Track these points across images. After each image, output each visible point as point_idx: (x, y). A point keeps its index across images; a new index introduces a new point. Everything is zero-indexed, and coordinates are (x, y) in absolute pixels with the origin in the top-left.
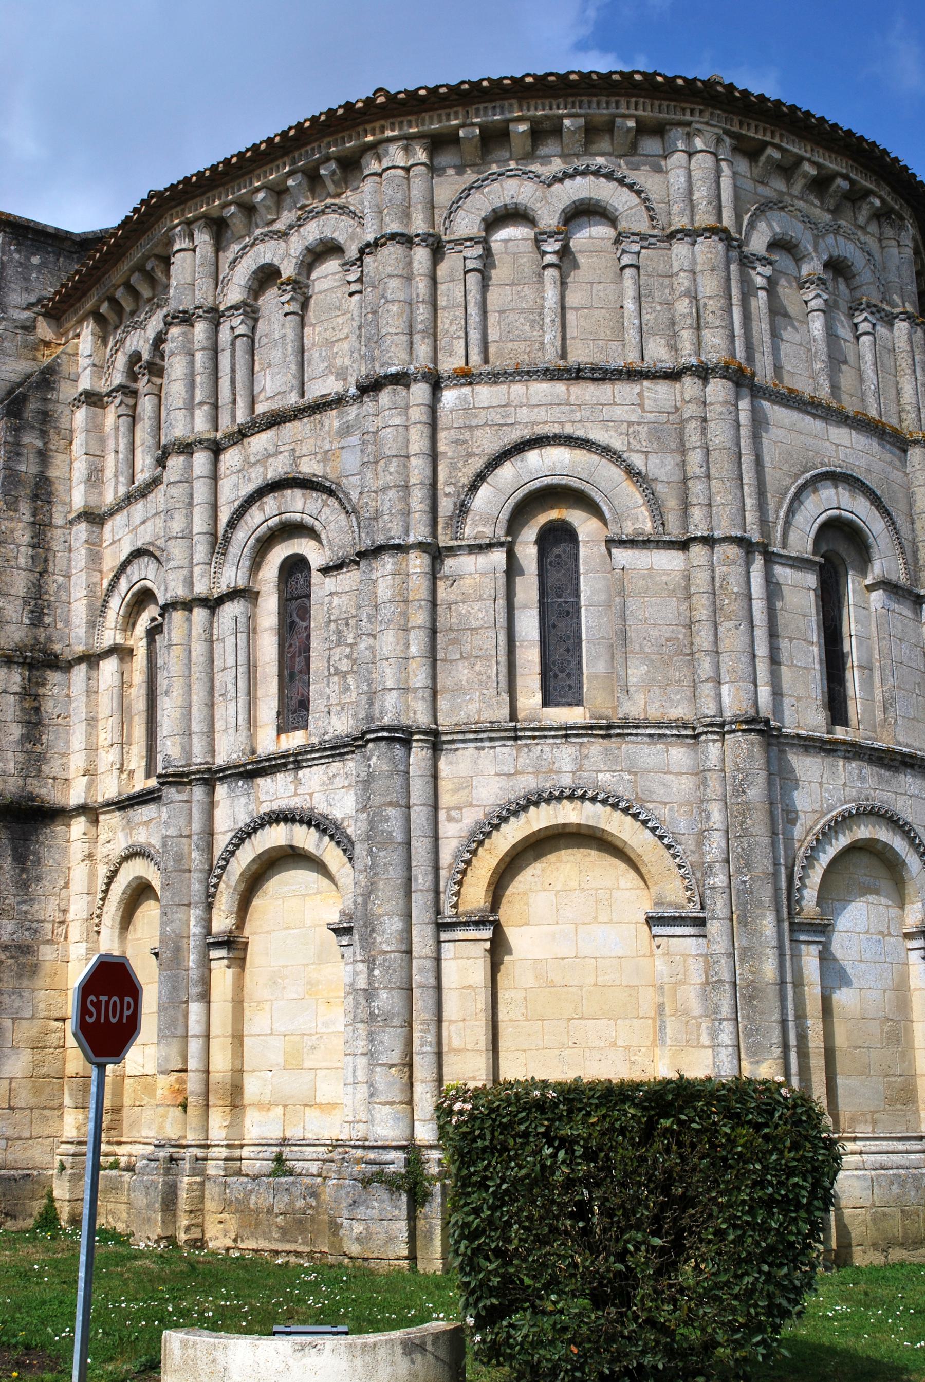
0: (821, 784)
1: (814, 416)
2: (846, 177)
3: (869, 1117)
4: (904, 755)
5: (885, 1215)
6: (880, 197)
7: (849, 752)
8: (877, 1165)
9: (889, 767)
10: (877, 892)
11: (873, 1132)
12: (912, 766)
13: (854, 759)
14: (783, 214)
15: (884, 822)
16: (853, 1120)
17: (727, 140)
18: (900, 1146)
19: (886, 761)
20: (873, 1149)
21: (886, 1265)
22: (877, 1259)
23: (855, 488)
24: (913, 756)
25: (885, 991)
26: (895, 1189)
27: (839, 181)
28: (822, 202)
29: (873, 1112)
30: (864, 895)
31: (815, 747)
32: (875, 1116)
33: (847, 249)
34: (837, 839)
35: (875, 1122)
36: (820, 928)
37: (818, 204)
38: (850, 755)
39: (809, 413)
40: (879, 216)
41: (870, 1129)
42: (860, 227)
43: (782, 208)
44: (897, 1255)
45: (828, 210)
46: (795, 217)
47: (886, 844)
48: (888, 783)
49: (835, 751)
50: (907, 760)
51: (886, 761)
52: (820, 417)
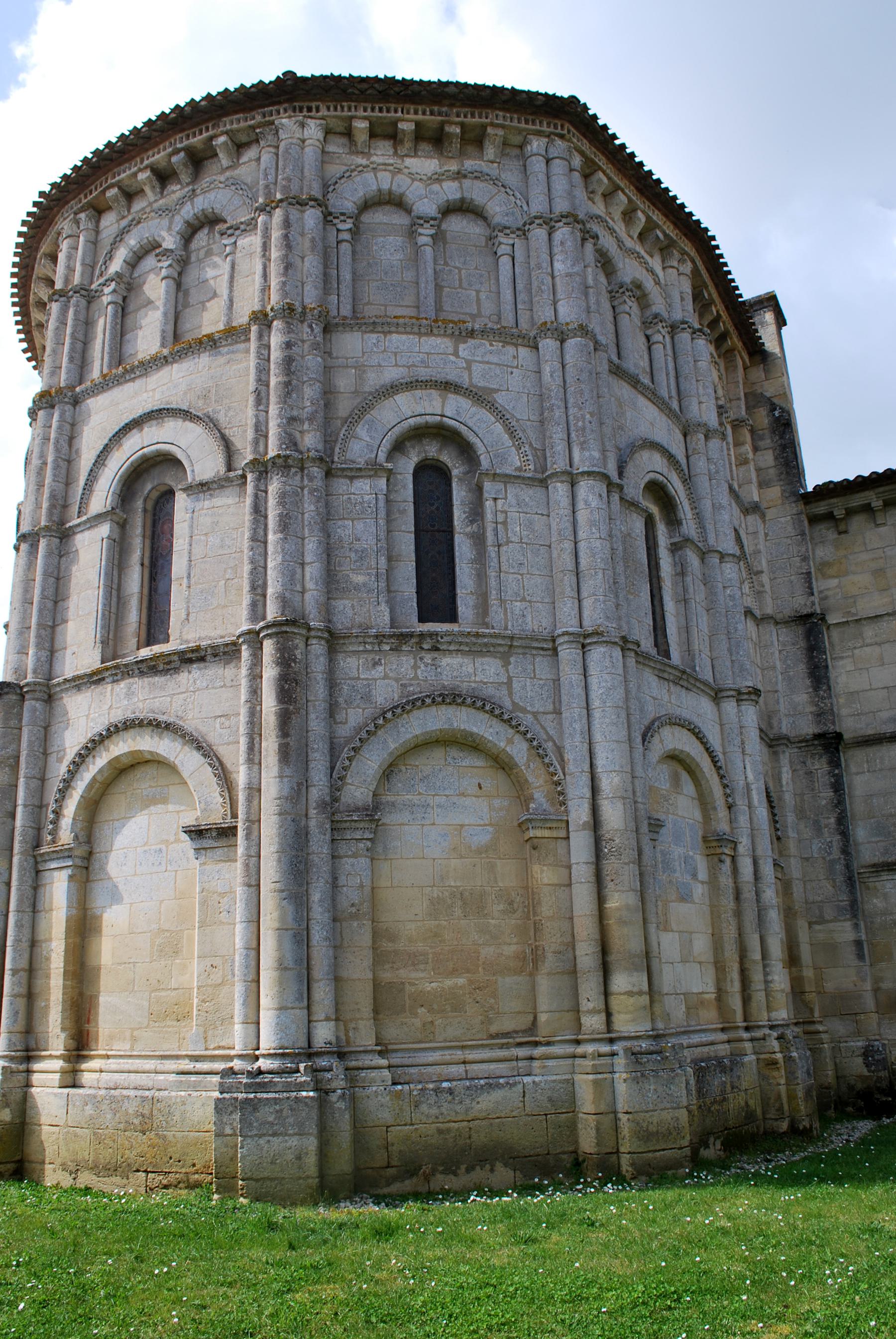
0: (88, 716)
1: (133, 380)
2: (176, 152)
3: (128, 1034)
4: (183, 652)
5: (76, 1135)
6: (222, 133)
7: (116, 674)
8: (112, 1085)
9: (165, 672)
10: (164, 801)
11: (132, 1049)
12: (202, 659)
13: (122, 679)
14: (140, 226)
15: (132, 732)
16: (112, 1037)
17: (82, 216)
18: (150, 1064)
19: (161, 667)
20: (127, 1067)
21: (73, 1189)
22: (66, 1181)
23: (162, 418)
24: (197, 649)
25: (161, 902)
26: (89, 1110)
27: (174, 159)
28: (179, 182)
29: (133, 1029)
30: (147, 806)
31: (85, 683)
32: (136, 1033)
33: (201, 203)
34: (94, 764)
35: (134, 1040)
36: (66, 854)
37: (179, 186)
38: (119, 677)
39: (129, 381)
40: (239, 147)
41: (128, 1047)
42: (227, 168)
43: (139, 222)
44: (86, 1179)
45: (188, 184)
46: (152, 218)
47: (132, 753)
48: (162, 688)
49: (103, 679)
50: (189, 655)
51: (161, 667)
52: (140, 376)
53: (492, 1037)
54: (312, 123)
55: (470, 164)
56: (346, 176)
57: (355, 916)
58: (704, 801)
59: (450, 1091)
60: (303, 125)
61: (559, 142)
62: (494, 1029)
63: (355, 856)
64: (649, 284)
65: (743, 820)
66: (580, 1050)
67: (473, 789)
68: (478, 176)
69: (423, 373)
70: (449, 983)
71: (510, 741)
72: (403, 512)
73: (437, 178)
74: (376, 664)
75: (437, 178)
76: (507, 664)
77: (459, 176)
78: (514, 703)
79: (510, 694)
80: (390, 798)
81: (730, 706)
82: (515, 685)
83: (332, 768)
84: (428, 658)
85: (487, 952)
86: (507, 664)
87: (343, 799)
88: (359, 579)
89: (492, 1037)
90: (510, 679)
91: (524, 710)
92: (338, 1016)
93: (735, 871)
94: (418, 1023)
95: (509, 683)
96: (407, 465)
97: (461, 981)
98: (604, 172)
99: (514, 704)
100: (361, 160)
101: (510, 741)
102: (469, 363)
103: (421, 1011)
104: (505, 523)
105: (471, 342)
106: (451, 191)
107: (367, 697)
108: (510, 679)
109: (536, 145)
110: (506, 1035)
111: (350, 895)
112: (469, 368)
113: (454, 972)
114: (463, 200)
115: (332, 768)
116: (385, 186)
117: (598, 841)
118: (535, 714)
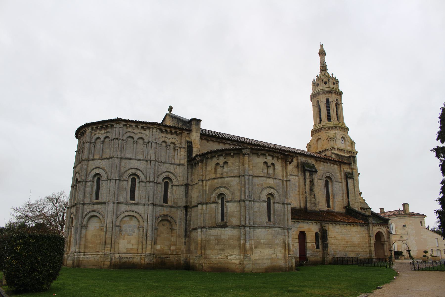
53: (96, 252)
54: (90, 129)
55: (108, 130)
56: (94, 135)
57: (83, 237)
58: (138, 221)
59: (87, 257)
60: (89, 129)
61: (117, 125)
62: (96, 251)
63: (84, 230)
64: (143, 136)
65: (146, 223)
66: (138, 255)
67: (98, 222)
68: (108, 132)
69: (97, 166)
70: (92, 245)
71: (100, 216)
72: (95, 185)
73: (104, 133)
74: (88, 207)
75: (104, 133)
76: (101, 206)
77: (106, 133)
78: (101, 211)
79: (101, 210)
80: (89, 223)
81: (146, 206)
82: (102, 209)
83: (82, 219)
84: (93, 205)
85: (97, 242)
86: (101, 206)
87: (83, 223)
88: (87, 196)
89: (96, 252)
90: (101, 208)
91: (102, 212)
92: (80, 248)
93: (143, 232)
94: (89, 249)
95: (101, 208)
96: (96, 179)
97: (93, 245)
98: (128, 124)
99: (101, 211)
100: (96, 133)
101: (100, 216)
102: (102, 163)
103: (89, 248)
104: (103, 187)
105: (103, 160)
106: (105, 135)
107: (86, 211)
108: (101, 208)
109: (115, 126)
110: (97, 252)
111: (82, 235)
112: (102, 164)
113: (93, 244)
114: (107, 136)
115: (82, 219)
116: (98, 136)
117: (106, 229)
118: (104, 212)
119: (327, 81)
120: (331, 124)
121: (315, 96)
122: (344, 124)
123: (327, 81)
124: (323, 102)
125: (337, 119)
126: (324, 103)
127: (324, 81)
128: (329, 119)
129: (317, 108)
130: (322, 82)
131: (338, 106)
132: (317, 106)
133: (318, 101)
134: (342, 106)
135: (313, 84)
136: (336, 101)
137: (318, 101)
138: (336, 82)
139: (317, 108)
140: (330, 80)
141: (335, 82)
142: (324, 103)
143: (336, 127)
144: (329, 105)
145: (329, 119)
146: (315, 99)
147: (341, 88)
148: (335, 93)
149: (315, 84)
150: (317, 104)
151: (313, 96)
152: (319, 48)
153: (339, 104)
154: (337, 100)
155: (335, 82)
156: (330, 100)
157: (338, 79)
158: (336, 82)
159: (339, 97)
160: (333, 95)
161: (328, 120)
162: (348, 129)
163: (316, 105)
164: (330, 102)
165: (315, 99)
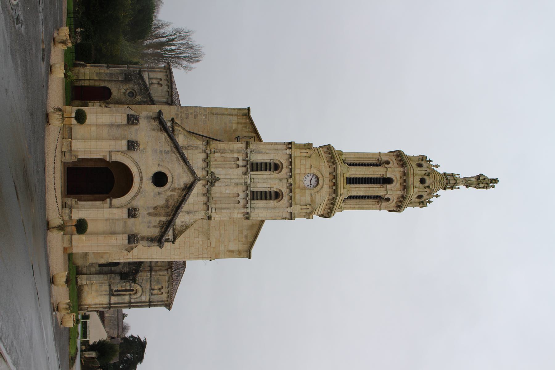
119: (426, 184)
120: (342, 182)
121: (400, 158)
122: (341, 209)
123: (426, 184)
124: (386, 172)
125: (350, 197)
126: (384, 173)
127: (426, 177)
128: (351, 181)
129: (375, 159)
130: (425, 174)
131: (376, 201)
132: (378, 160)
133: (388, 163)
134: (376, 208)
135: (423, 158)
136: (386, 196)
137: (388, 163)
138: (422, 202)
139: (375, 161)
140: (427, 189)
141: (422, 200)
142: (384, 173)
143: (335, 192)
144: (380, 184)
145: (351, 181)
146: (394, 158)
147: (409, 211)
148: (403, 197)
149: (422, 161)
150: (382, 161)
151: (399, 155)
152: (490, 176)
153: (380, 203)
154: (388, 200)
155: (422, 200)
156: (389, 186)
157: (427, 206)
158: (422, 202)
159: (393, 204)
160: (399, 193)
161: (350, 178)
162: (329, 217)
163: (380, 159)
164: (385, 185)
165: (393, 159)
